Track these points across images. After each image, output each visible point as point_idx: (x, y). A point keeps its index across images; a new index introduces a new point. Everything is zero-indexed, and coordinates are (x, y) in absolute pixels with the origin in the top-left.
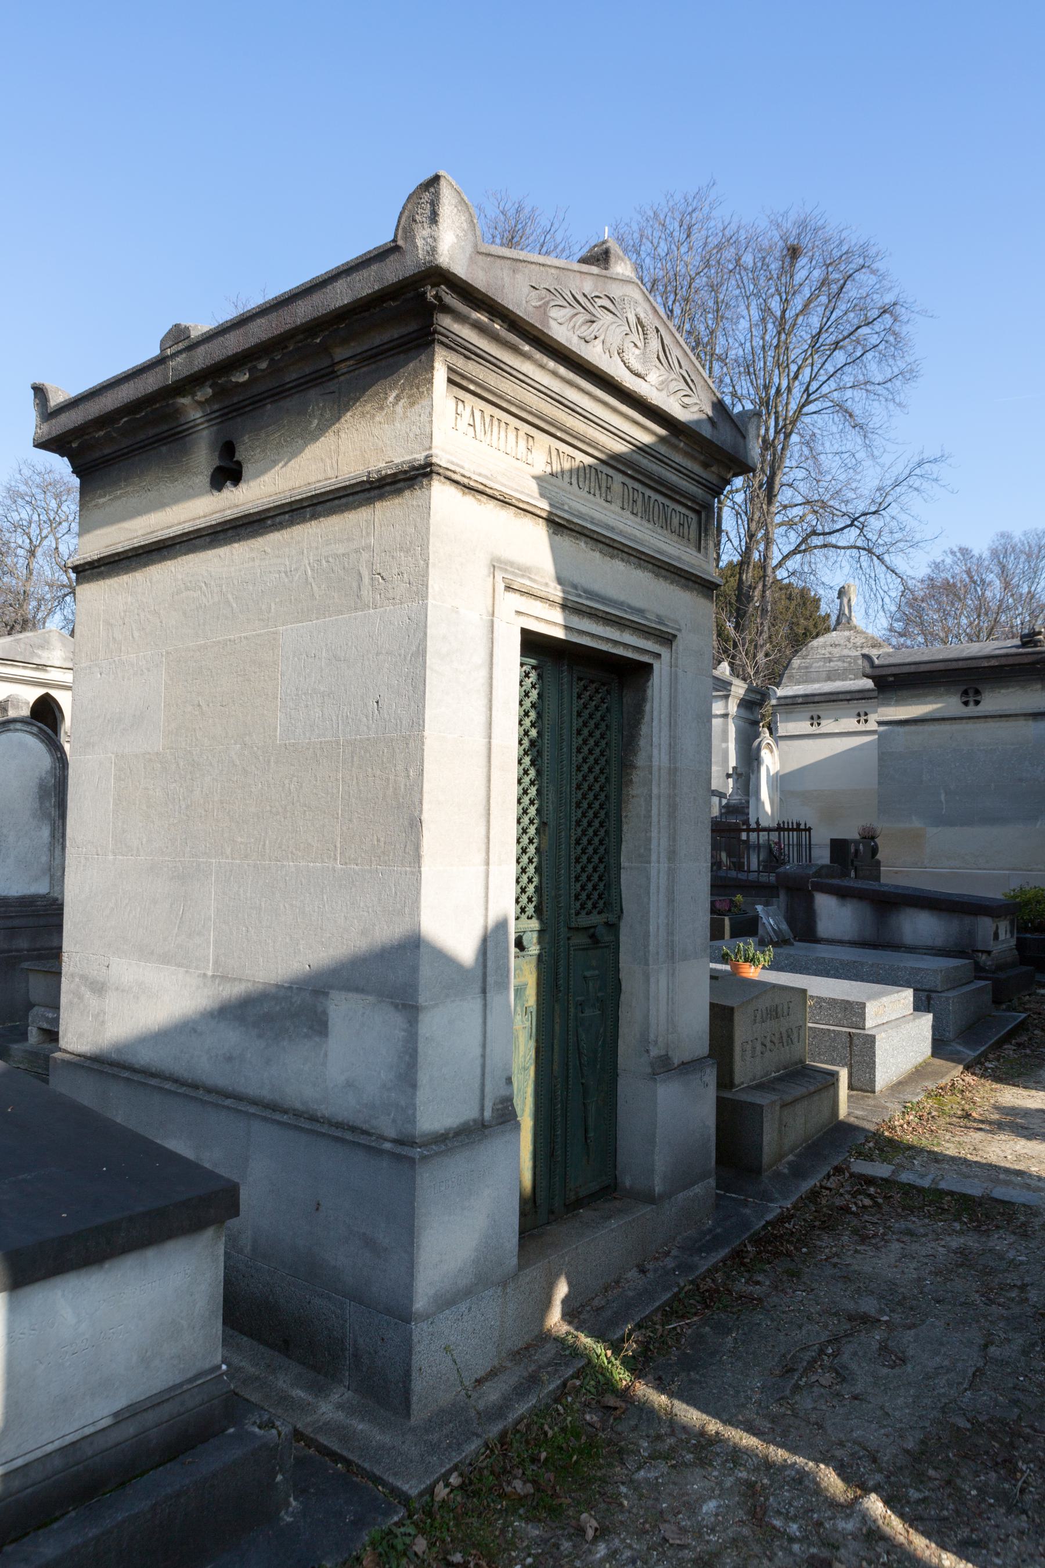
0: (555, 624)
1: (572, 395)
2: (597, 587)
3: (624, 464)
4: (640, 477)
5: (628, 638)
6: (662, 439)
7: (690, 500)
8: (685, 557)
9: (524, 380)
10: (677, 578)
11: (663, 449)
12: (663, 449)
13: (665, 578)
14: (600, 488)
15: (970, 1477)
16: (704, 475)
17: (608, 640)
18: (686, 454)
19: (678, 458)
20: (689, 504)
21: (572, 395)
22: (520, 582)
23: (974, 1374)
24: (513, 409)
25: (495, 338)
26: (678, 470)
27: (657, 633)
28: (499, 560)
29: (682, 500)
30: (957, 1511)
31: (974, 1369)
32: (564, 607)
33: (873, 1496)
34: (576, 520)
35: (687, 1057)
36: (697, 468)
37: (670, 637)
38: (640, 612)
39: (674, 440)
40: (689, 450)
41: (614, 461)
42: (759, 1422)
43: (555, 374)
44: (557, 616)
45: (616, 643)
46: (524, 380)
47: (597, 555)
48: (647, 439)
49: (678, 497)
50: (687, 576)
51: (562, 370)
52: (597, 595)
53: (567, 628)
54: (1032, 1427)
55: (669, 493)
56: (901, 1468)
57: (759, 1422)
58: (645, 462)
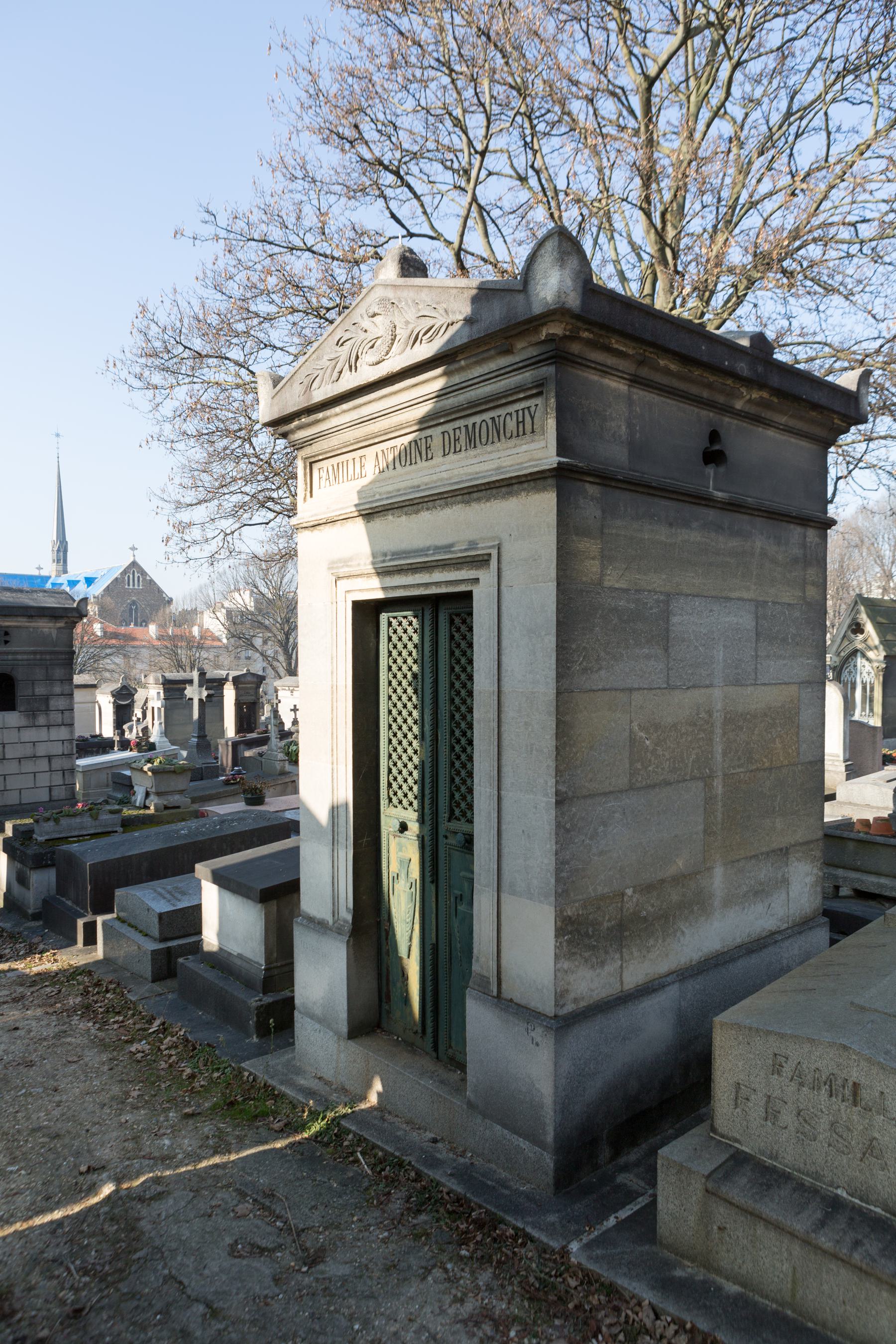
0: (373, 589)
1: (366, 411)
2: (404, 546)
3: (432, 419)
4: (454, 416)
5: (438, 576)
6: (445, 374)
7: (519, 392)
8: (506, 462)
9: (338, 430)
10: (494, 491)
11: (456, 379)
12: (456, 379)
13: (478, 500)
14: (420, 454)
15: (99, 1247)
16: (517, 359)
17: (419, 585)
18: (479, 363)
19: (477, 371)
20: (522, 395)
21: (366, 411)
22: (343, 571)
23: (181, 1283)
24: (344, 450)
25: (309, 425)
26: (485, 379)
27: (468, 559)
28: (333, 562)
29: (510, 399)
30: (83, 1231)
31: (186, 1284)
32: (378, 574)
33: (113, 1188)
34: (374, 505)
35: (517, 997)
36: (503, 361)
37: (486, 558)
38: (448, 548)
39: (456, 366)
40: (474, 359)
41: (425, 423)
42: (220, 1172)
43: (344, 412)
44: (375, 582)
45: (427, 585)
46: (338, 430)
47: (404, 518)
48: (439, 384)
49: (504, 401)
50: (505, 483)
51: (345, 406)
52: (404, 552)
53: (384, 589)
54: (107, 1296)
55: (492, 405)
56: (127, 1211)
57: (220, 1172)
58: (451, 401)
